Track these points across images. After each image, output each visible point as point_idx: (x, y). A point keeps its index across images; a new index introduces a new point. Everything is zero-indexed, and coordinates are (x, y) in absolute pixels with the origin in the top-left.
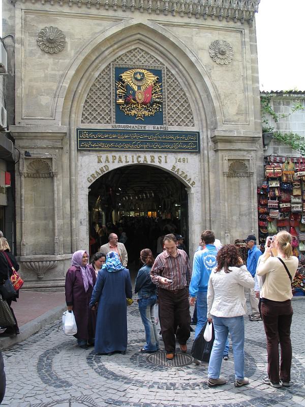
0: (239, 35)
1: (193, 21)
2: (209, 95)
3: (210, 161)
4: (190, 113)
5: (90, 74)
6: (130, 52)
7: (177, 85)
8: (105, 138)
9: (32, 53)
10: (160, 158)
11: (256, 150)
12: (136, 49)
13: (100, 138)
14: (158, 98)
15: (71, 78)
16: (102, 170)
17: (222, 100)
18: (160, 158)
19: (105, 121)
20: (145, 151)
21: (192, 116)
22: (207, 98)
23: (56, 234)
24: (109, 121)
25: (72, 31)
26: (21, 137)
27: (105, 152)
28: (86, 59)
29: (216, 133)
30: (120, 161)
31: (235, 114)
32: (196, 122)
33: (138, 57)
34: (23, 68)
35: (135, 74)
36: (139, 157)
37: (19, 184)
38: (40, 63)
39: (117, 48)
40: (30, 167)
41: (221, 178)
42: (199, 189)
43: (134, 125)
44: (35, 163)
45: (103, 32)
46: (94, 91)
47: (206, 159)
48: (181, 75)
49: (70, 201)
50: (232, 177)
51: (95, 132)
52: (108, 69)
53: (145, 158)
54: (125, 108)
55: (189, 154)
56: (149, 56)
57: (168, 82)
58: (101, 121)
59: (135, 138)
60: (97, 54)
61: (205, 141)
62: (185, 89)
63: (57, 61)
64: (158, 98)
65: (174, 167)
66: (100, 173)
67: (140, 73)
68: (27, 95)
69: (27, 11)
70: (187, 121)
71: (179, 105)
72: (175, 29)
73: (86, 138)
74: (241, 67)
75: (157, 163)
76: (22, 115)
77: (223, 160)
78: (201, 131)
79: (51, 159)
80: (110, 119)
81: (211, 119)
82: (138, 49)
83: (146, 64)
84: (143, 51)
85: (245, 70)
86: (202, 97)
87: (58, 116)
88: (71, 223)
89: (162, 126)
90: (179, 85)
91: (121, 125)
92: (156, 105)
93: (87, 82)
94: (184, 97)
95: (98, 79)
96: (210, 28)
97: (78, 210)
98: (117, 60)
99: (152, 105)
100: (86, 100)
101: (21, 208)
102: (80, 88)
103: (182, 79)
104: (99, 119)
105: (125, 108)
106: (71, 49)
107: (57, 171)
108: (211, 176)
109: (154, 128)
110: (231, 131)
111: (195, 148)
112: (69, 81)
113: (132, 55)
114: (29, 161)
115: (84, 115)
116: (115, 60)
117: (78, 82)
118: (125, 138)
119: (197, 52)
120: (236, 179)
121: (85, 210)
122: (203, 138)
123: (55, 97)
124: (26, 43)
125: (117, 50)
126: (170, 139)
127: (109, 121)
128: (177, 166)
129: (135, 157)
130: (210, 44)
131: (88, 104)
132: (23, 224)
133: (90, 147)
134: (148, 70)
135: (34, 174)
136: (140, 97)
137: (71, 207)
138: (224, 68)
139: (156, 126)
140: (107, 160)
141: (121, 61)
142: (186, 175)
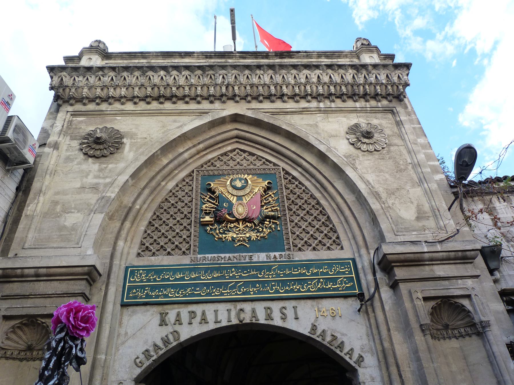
0: (390, 116)
1: (314, 104)
3: (387, 308)
4: (334, 230)
6: (225, 154)
8: (176, 280)
10: (284, 310)
11: (477, 277)
12: (234, 150)
13: (168, 280)
16: (166, 341)
18: (284, 310)
21: (336, 235)
24: (187, 252)
25: (134, 130)
27: (176, 306)
28: (150, 162)
29: (386, 249)
30: (204, 320)
31: (414, 218)
32: (345, 243)
33: (238, 160)
34: (48, 176)
38: (77, 170)
39: (206, 149)
40: (13, 336)
41: (419, 337)
43: (231, 255)
44: (26, 329)
45: (181, 126)
48: (307, 175)
50: (444, 338)
51: (158, 271)
52: (191, 178)
53: (254, 311)
54: (215, 229)
55: (342, 299)
56: (255, 158)
58: (172, 252)
59: (234, 277)
60: (171, 156)
62: (318, 195)
63: (105, 166)
64: (272, 211)
65: (314, 328)
68: (45, 215)
69: (75, 114)
72: (288, 117)
73: (142, 281)
74: (405, 152)
75: (277, 322)
76: (25, 243)
77: (412, 300)
82: (237, 150)
83: (252, 167)
84: (244, 151)
85: (413, 154)
89: (283, 253)
90: (307, 191)
91: (207, 255)
92: (270, 222)
94: (317, 206)
96: (340, 111)
98: (205, 166)
99: (262, 222)
100: (150, 222)
102: (140, 201)
103: (310, 181)
104: (169, 250)
105: (215, 229)
106: (130, 151)
109: (268, 257)
111: (353, 288)
112: (117, 190)
113: (228, 158)
117: (136, 195)
118: (214, 278)
119: (328, 140)
120: (454, 343)
122: (363, 268)
124: (63, 147)
125: (204, 153)
126: (300, 275)
127: (187, 252)
129: (233, 314)
130: (346, 129)
131: (153, 228)
133: (148, 296)
136: (240, 211)
138: (377, 157)
139: (272, 254)
140: (178, 321)
141: (212, 168)
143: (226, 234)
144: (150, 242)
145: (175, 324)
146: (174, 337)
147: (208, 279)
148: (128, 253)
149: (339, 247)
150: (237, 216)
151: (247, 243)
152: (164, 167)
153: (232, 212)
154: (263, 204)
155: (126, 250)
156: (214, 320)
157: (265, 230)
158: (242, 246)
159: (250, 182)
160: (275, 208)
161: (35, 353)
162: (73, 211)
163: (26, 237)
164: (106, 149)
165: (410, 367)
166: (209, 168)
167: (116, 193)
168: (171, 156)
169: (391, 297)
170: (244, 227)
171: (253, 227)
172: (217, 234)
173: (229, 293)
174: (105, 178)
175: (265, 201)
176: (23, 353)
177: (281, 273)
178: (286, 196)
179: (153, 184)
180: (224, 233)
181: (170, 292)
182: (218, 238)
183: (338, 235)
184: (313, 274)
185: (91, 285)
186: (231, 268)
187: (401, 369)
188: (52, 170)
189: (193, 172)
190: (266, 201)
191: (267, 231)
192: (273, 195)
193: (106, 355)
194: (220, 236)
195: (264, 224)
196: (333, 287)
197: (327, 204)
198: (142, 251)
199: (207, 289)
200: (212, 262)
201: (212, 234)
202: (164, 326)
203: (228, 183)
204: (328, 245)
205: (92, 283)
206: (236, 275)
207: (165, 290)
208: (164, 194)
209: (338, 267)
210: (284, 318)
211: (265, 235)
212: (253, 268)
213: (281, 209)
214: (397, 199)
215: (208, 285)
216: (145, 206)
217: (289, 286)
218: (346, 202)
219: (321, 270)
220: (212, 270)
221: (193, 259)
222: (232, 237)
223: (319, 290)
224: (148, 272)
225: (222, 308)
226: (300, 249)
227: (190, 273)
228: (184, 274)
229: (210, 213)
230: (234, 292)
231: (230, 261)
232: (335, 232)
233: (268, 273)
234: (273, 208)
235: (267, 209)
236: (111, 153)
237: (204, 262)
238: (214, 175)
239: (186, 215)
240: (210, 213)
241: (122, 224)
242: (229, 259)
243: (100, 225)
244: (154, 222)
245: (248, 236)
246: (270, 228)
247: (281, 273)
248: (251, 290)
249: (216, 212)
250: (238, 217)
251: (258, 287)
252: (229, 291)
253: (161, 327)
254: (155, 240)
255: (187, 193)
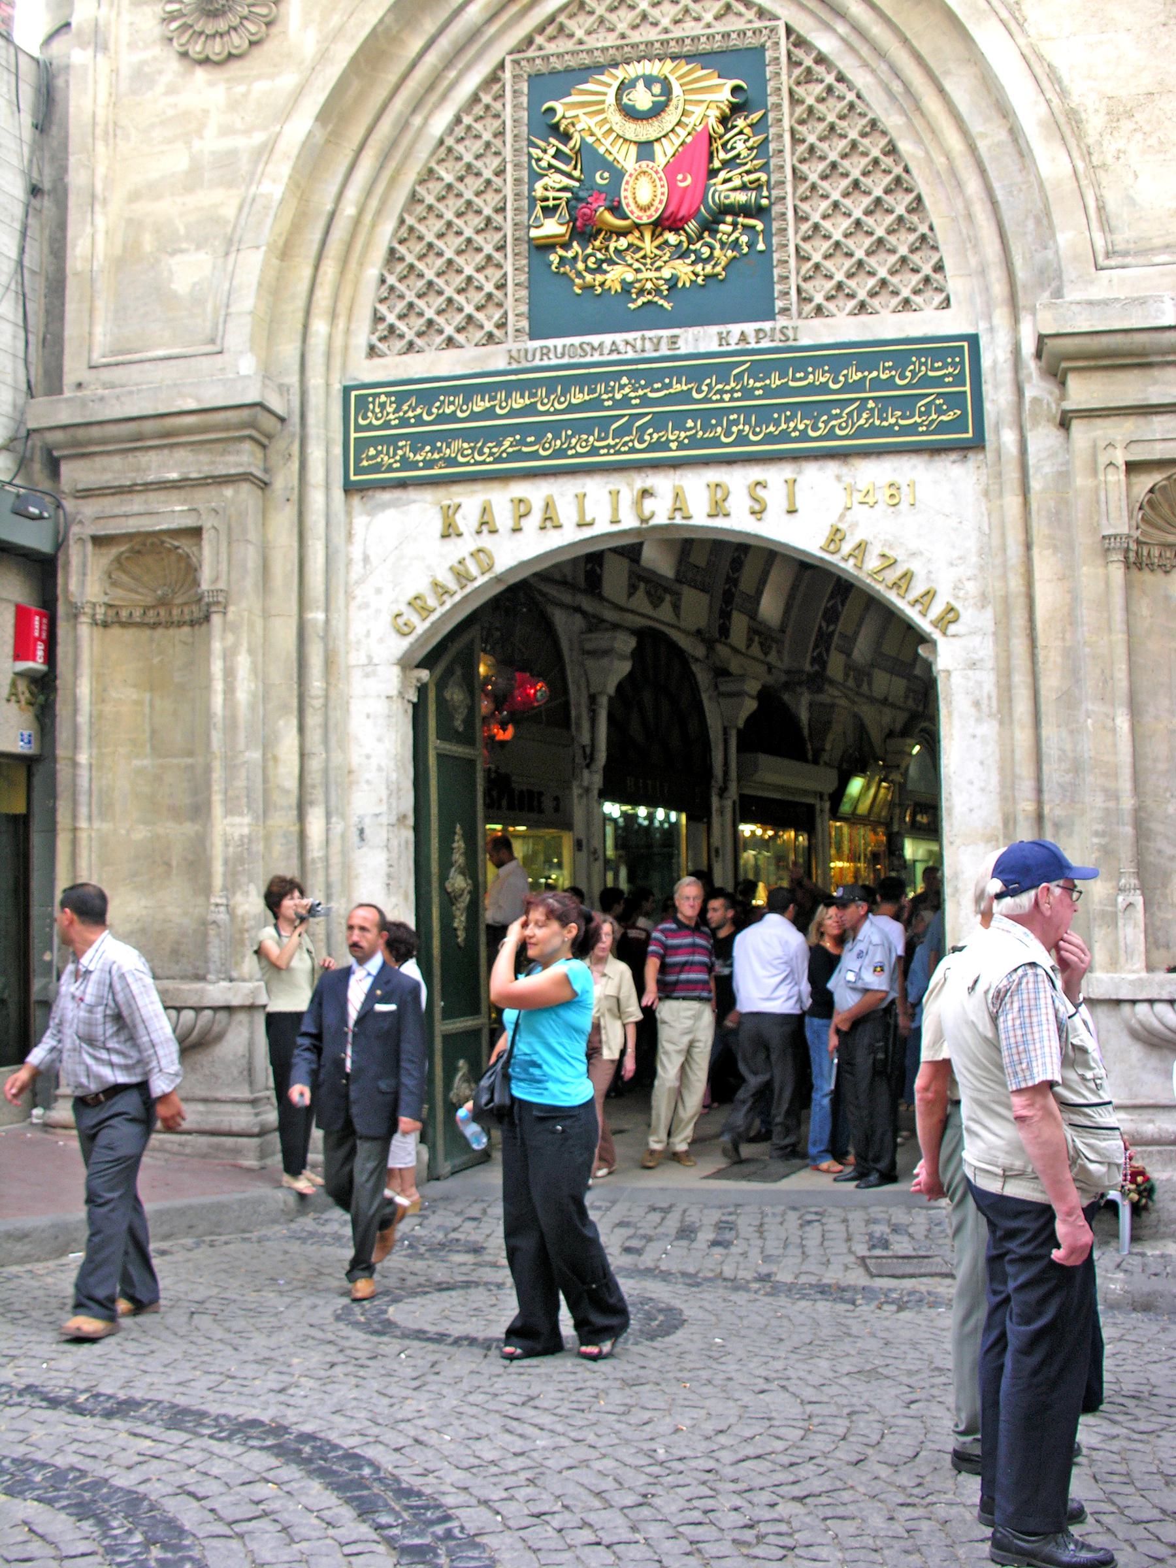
2: (1015, 133)
3: (1036, 485)
5: (403, 126)
7: (851, 106)
8: (474, 416)
9: (142, 77)
10: (760, 492)
13: (452, 418)
14: (744, 187)
15: (294, 152)
17: (1090, 141)
18: (760, 492)
19: (479, 335)
20: (676, 465)
21: (935, 258)
22: (1010, 148)
23: (218, 881)
26: (91, 442)
27: (478, 487)
30: (550, 521)
34: (100, 148)
35: (624, 87)
36: (646, 493)
37: (71, 657)
38: (171, 112)
40: (125, 578)
42: (985, 648)
43: (619, 338)
46: (430, 200)
47: (1012, 474)
48: (865, 51)
49: (301, 729)
52: (496, 87)
55: (926, 457)
57: (795, 101)
58: (460, 338)
59: (625, 402)
60: (429, 26)
61: (1007, 376)
62: (892, 121)
64: (744, 187)
65: (836, 536)
66: (452, 585)
67: (649, 81)
70: (906, 283)
71: (858, 207)
73: (387, 425)
76: (90, 351)
78: (981, 329)
79: (196, 533)
80: (501, 325)
81: (1038, 257)
83: (690, 28)
86: (982, 146)
87: (237, 336)
88: (302, 836)
89: (767, 325)
90: (860, 107)
91: (550, 343)
92: (735, 225)
93: (392, 165)
94: (887, 162)
95: (450, 141)
97: (350, 772)
98: (539, 40)
99: (709, 226)
100: (392, 251)
101: (75, 764)
102: (353, 193)
105: (575, 258)
107: (221, 585)
108: (1045, 566)
109: (721, 338)
110: (1142, 302)
111: (958, 425)
114: (114, 551)
115: (382, 319)
116: (529, 41)
118: (572, 408)
121: (380, 769)
122: (995, 362)
123: (227, 254)
128: (854, 525)
131: (400, 268)
132: (83, 836)
133: (406, 464)
134: (689, 58)
135: (146, 609)
137: (302, 755)
139: (736, 329)
140: (486, 524)
142: (908, 576)
143: (606, 272)
144: (397, 310)
145: (479, 532)
146: (479, 563)
147: (557, 412)
148: (346, 348)
149: (939, 298)
150: (636, 215)
151: (665, 298)
152: (413, 65)
153: (619, 202)
154: (717, 164)
155: (338, 342)
156: (575, 519)
157: (717, 253)
158: (652, 308)
159: (677, 90)
160: (753, 177)
161: (176, 612)
162: (184, 246)
163: (90, 334)
164: (235, 29)
165: (1063, 639)
166: (551, 48)
167: (285, 180)
168: (429, 26)
169: (1053, 455)
170: (658, 248)
171: (685, 245)
172: (579, 275)
173: (614, 447)
174: (247, 132)
175: (722, 155)
176: (151, 613)
177: (758, 385)
178: (793, 132)
179: (385, 127)
180: (599, 270)
181: (461, 451)
182: (583, 288)
183: (941, 259)
184: (847, 389)
185: (264, 447)
186: (617, 376)
187: (1041, 642)
188: (107, 125)
189: (502, 66)
190: (727, 152)
191: (723, 256)
192: (747, 130)
193: (327, 610)
194: (589, 277)
195: (717, 231)
196: (901, 422)
197: (921, 154)
198: (382, 339)
199: (557, 436)
200: (566, 360)
201: (565, 274)
202: (454, 540)
203: (611, 99)
204: (906, 292)
205: (265, 441)
206: (632, 395)
207: (448, 446)
208: (423, 153)
209: (925, 364)
210: (758, 513)
211: (718, 269)
212: (677, 372)
213: (774, 178)
214: (1139, 136)
215: (556, 428)
216: (374, 203)
217: (777, 424)
218: (973, 149)
219: (875, 374)
220: (567, 383)
221: (514, 354)
222: (623, 282)
223: (860, 433)
224: (401, 398)
225: (596, 488)
226: (819, 310)
227: (508, 396)
228: (492, 399)
229: (556, 207)
230: (625, 444)
231: (614, 357)
232: (935, 248)
233: (720, 386)
234: (746, 178)
235: (729, 180)
236: (252, 44)
237: (546, 362)
238: (569, 70)
239: (489, 220)
240: (556, 207)
241: (317, 268)
242: (614, 349)
243: (260, 284)
244: (402, 250)
245: (668, 276)
246: (736, 245)
247: (758, 385)
248: (672, 437)
249: (573, 203)
250: (639, 218)
251: (691, 429)
252: (612, 443)
253: (447, 540)
254: (411, 305)
255: (488, 145)
